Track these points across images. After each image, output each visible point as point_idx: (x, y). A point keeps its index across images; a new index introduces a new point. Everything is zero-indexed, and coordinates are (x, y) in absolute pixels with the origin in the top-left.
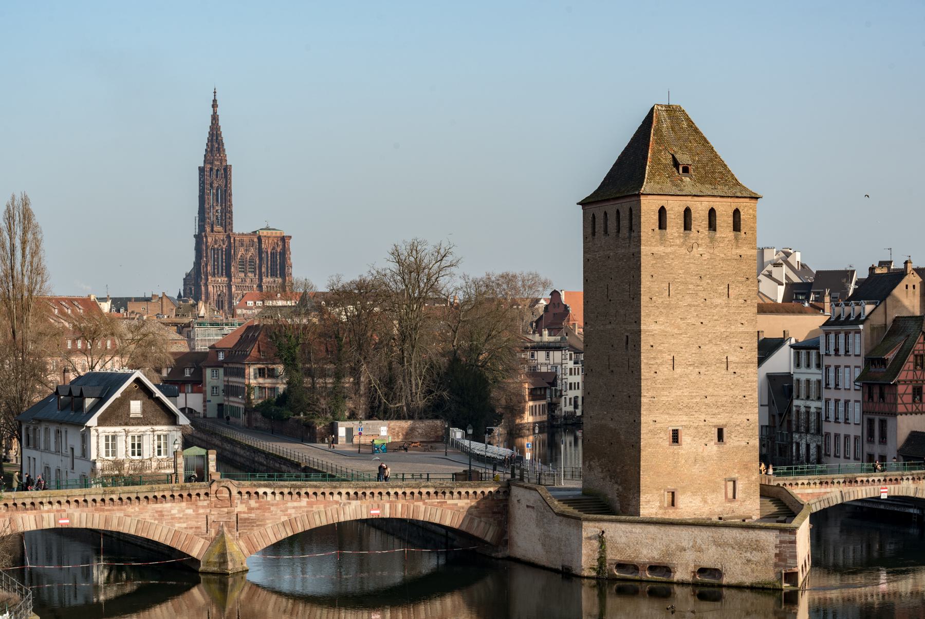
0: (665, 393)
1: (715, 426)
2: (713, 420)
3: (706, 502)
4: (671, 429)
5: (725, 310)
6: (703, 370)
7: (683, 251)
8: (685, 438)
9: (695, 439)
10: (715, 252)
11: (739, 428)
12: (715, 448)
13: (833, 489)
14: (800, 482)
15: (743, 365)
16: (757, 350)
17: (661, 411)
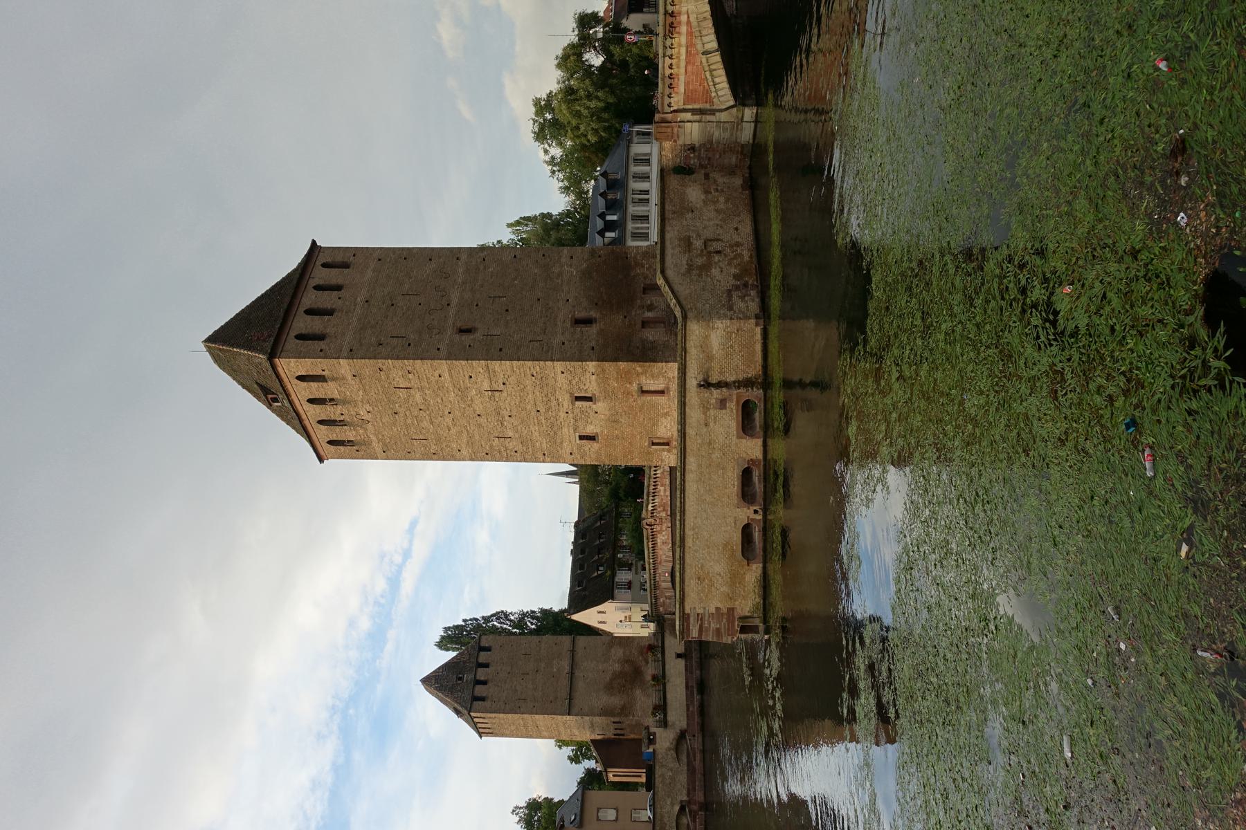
0: (538, 444)
1: (573, 404)
2: (566, 405)
3: (667, 414)
4: (578, 442)
5: (427, 392)
6: (506, 413)
7: (369, 426)
8: (590, 430)
9: (589, 421)
10: (360, 399)
11: (574, 382)
12: (600, 404)
13: (684, 9)
14: (668, 72)
15: (492, 376)
16: (470, 362)
17: (559, 449)
